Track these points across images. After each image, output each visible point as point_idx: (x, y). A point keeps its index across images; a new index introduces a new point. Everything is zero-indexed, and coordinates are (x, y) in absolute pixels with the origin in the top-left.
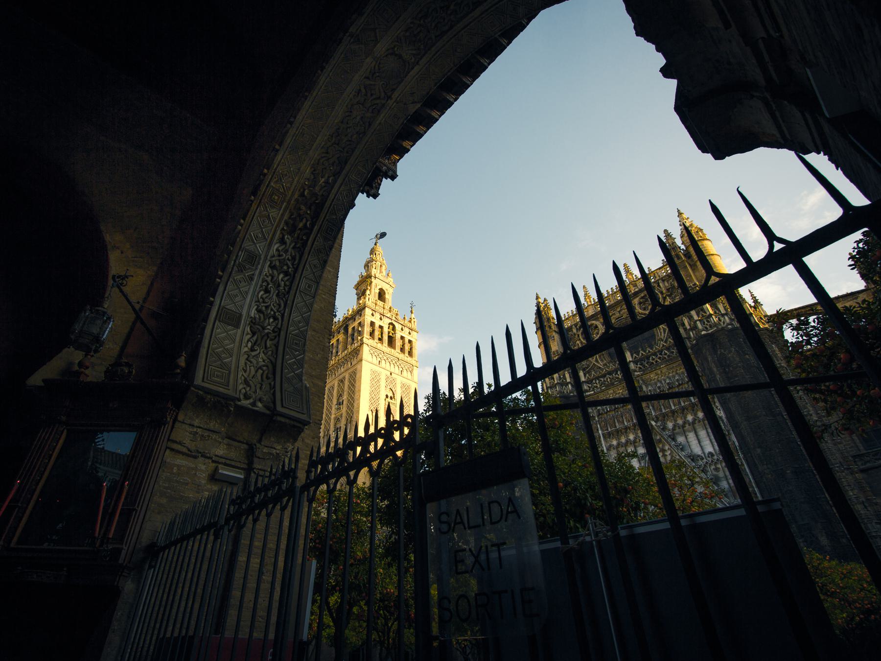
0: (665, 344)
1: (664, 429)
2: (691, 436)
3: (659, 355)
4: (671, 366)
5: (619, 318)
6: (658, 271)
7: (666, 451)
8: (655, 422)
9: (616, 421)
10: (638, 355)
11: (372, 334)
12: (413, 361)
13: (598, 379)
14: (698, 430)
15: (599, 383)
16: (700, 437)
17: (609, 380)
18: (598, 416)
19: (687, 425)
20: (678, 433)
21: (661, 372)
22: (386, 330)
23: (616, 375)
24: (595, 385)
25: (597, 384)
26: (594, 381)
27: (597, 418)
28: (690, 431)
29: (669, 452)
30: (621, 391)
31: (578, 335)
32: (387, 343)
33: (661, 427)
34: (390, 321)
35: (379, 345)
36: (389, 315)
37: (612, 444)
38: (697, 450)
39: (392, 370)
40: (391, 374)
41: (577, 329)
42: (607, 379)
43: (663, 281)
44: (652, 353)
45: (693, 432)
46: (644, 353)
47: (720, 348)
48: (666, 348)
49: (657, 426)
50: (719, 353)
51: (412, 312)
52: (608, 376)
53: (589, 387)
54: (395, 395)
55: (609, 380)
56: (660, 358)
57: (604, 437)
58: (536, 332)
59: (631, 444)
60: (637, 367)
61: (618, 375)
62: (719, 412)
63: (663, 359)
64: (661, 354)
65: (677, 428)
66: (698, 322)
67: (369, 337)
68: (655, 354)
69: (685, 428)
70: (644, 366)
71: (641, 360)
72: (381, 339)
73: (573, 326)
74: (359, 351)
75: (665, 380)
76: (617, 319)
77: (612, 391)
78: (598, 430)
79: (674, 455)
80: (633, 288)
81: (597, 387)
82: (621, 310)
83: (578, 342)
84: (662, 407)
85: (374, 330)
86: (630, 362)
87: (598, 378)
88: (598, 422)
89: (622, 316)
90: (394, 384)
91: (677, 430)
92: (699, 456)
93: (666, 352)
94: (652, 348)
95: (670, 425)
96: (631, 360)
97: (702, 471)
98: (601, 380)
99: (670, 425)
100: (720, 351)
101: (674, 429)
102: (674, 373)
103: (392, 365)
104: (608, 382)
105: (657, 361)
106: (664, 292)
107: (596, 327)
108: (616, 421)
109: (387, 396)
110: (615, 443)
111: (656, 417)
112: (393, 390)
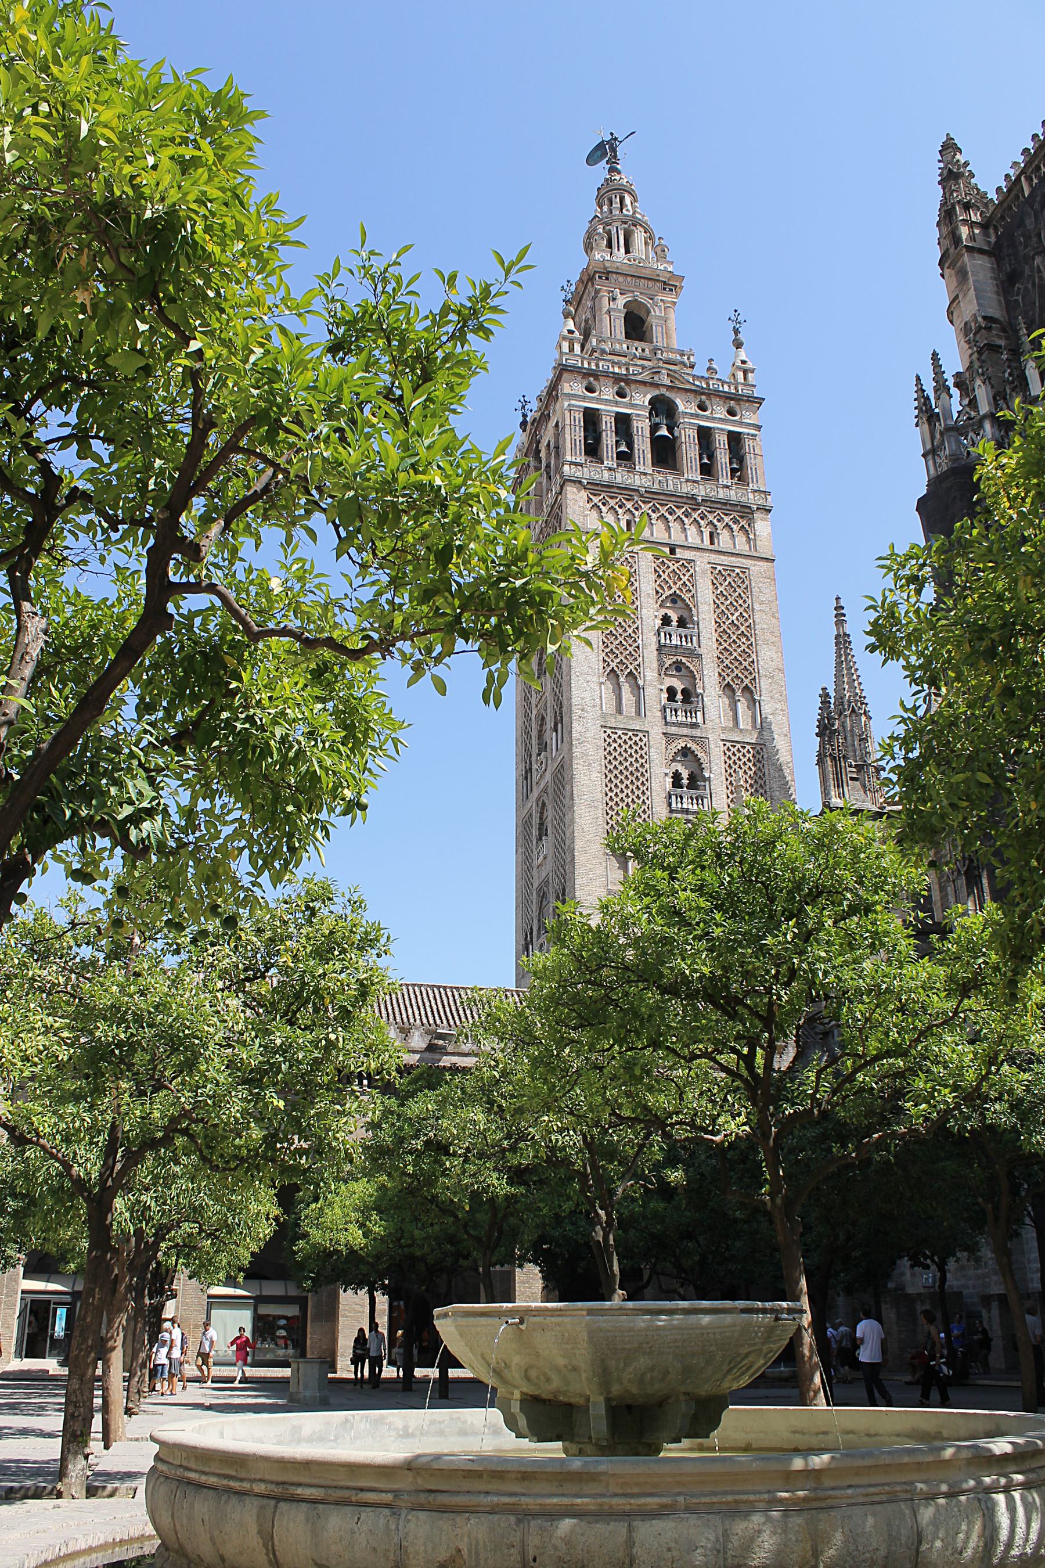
11: (593, 450)
12: (751, 496)
22: (641, 426)
32: (649, 461)
34: (657, 392)
35: (621, 477)
36: (645, 376)
39: (677, 538)
40: (672, 551)
51: (738, 345)
54: (694, 611)
67: (581, 459)
72: (625, 458)
74: (560, 508)
85: (598, 439)
90: (685, 579)
103: (675, 527)
109: (666, 621)
112: (686, 597)
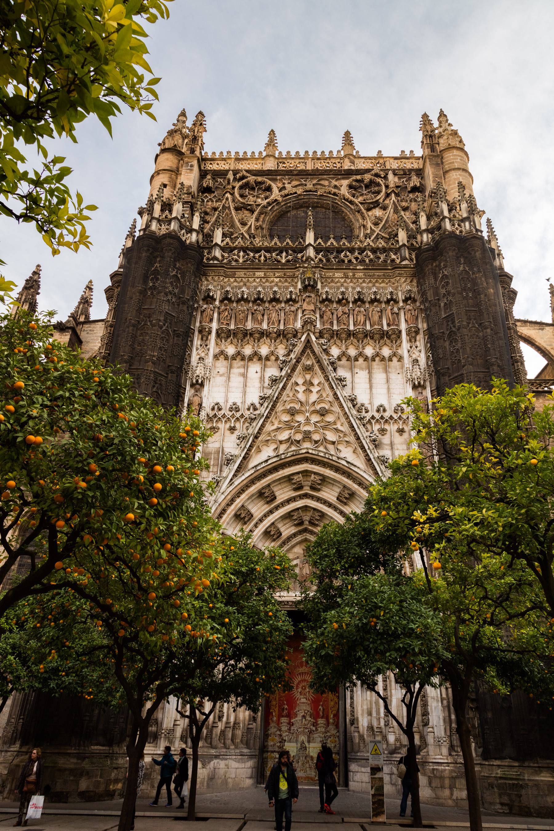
0: (371, 244)
1: (326, 351)
2: (362, 376)
3: (356, 254)
4: (371, 273)
5: (310, 191)
6: (392, 161)
7: (313, 385)
8: (316, 338)
9: (250, 318)
10: (325, 242)
13: (244, 251)
14: (374, 371)
15: (243, 257)
16: (374, 381)
17: (262, 258)
18: (221, 301)
19: (361, 360)
20: (343, 367)
21: (354, 275)
23: (277, 255)
24: (235, 257)
25: (239, 257)
26: (236, 252)
27: (217, 303)
28: (362, 369)
29: (318, 388)
30: (277, 280)
31: (234, 188)
33: (325, 347)
37: (226, 350)
38: (362, 398)
41: (235, 179)
42: (260, 256)
43: (395, 174)
44: (349, 248)
45: (367, 371)
46: (335, 243)
47: (464, 263)
48: (373, 248)
49: (318, 344)
50: (461, 268)
52: (263, 252)
53: (223, 256)
55: (262, 258)
56: (357, 258)
57: (218, 335)
58: (157, 156)
59: (260, 359)
60: (316, 258)
61: (281, 257)
62: (417, 354)
63: (360, 262)
64: (359, 253)
65: (344, 359)
66: (447, 220)
68: (352, 250)
69: (356, 363)
70: (328, 260)
71: (328, 250)
73: (231, 172)
75: (354, 288)
76: (306, 191)
77: (262, 274)
78: (211, 320)
79: (324, 395)
80: (349, 164)
81: (236, 261)
82: (316, 184)
83: (228, 195)
84: (335, 322)
86: (310, 245)
87: (245, 250)
88: (216, 309)
89: (316, 191)
91: (344, 361)
92: (363, 405)
93: (369, 253)
94: (350, 242)
95: (335, 352)
96: (312, 243)
97: (364, 425)
98: (248, 255)
99: (335, 352)
100: (464, 268)
101: (339, 359)
102: (370, 285)
104: (260, 261)
105: (350, 261)
106: (392, 185)
107: (269, 189)
108: (250, 318)
110: (231, 350)
111: (320, 332)
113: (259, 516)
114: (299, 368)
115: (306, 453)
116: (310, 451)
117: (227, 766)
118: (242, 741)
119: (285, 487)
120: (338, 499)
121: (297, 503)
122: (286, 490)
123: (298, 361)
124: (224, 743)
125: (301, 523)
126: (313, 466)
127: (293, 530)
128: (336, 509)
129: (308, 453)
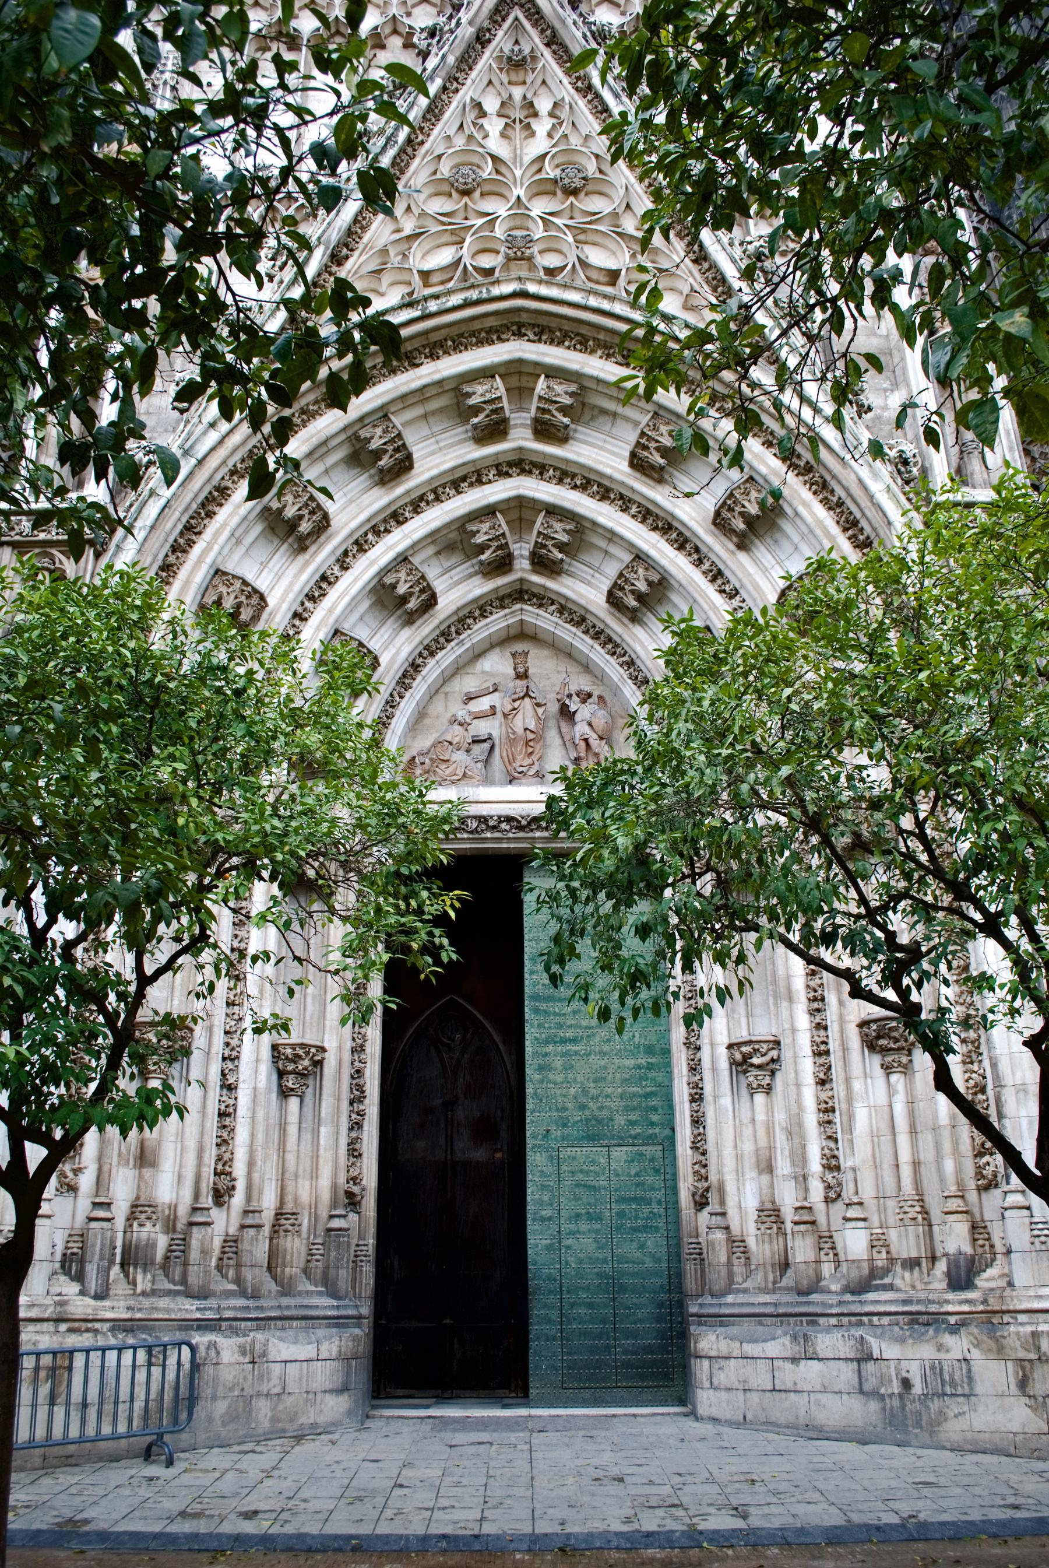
113: (353, 525)
114: (487, 58)
115: (515, 295)
116: (532, 288)
117: (256, 1358)
118: (306, 1271)
119: (445, 431)
120: (632, 465)
121: (487, 489)
122: (447, 438)
123: (481, 40)
124: (238, 1280)
125: (503, 564)
126: (542, 348)
127: (480, 587)
128: (625, 502)
129: (523, 294)
